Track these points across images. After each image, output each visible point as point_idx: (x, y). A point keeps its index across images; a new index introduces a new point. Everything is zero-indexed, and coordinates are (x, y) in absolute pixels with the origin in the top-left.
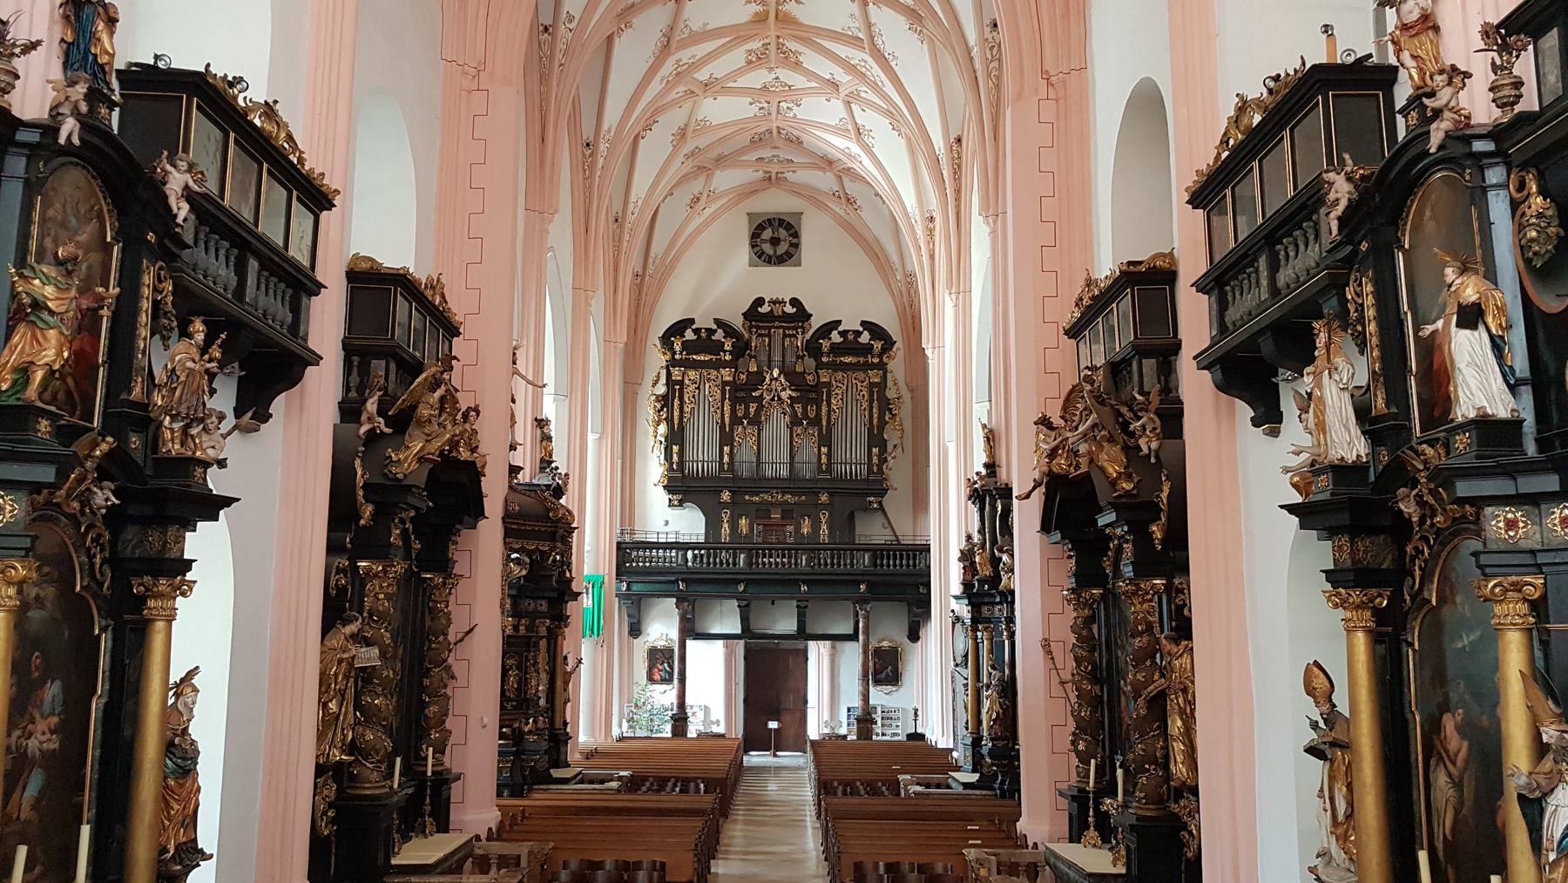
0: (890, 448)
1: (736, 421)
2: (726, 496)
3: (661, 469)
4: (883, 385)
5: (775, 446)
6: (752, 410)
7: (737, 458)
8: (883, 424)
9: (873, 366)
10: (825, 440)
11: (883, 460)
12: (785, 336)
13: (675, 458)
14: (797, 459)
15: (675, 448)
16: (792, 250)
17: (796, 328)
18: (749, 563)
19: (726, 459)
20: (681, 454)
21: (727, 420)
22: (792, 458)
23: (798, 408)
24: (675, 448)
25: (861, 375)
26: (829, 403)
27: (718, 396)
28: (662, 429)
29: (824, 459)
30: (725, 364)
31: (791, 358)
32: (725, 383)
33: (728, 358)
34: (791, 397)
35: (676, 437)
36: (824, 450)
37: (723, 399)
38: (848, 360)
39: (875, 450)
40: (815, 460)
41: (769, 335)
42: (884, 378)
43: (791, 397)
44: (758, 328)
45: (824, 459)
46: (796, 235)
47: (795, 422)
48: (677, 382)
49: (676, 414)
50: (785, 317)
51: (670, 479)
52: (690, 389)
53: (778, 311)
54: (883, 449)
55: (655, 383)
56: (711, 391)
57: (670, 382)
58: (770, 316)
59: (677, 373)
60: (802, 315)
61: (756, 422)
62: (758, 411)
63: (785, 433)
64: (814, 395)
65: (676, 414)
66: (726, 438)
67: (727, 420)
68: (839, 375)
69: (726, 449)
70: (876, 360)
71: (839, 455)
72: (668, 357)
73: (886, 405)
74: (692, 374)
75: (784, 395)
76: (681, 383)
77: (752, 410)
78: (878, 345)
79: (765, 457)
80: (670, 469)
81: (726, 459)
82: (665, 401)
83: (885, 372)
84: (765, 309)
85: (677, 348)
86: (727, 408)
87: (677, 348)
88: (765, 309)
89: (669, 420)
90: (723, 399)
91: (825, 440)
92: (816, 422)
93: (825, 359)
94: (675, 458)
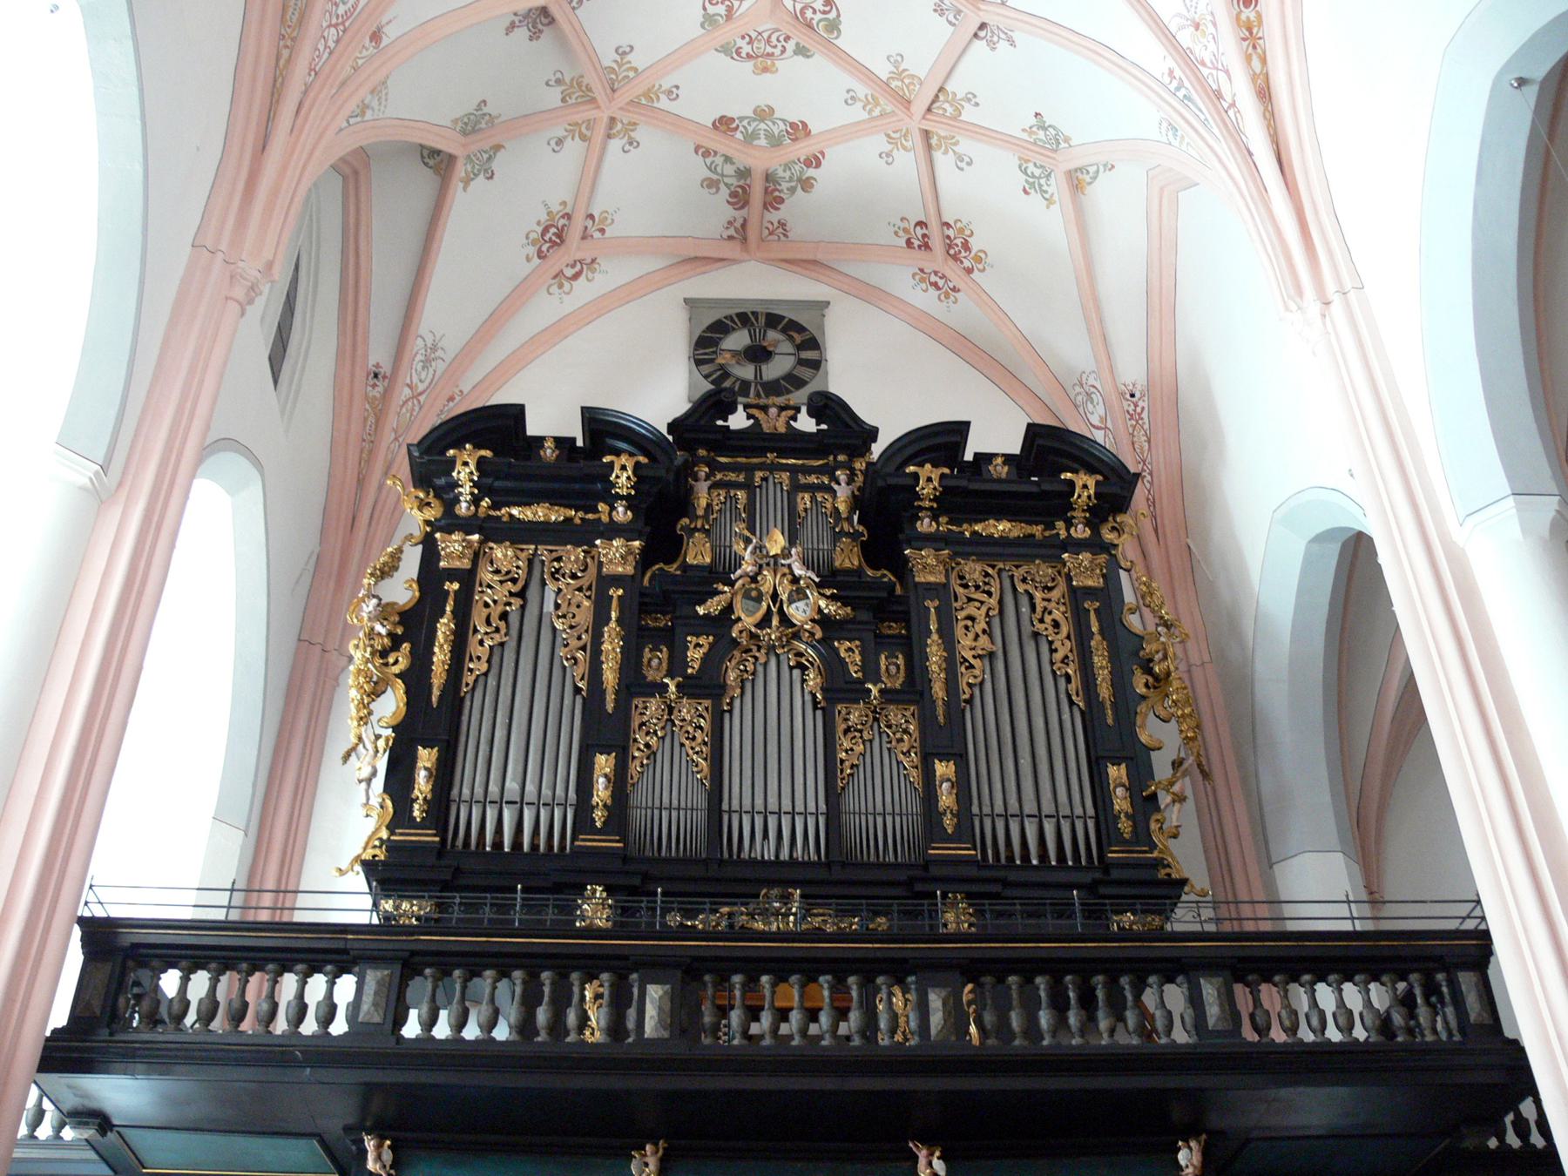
0: (1161, 765)
1: (635, 684)
2: (595, 908)
3: (371, 824)
4: (1108, 595)
5: (775, 763)
6: (695, 656)
7: (640, 797)
8: (1126, 703)
9: (1076, 546)
10: (944, 738)
11: (1146, 804)
12: (796, 488)
13: (422, 784)
14: (851, 802)
15: (426, 757)
16: (804, 372)
17: (830, 471)
18: (682, 1016)
19: (601, 791)
20: (444, 775)
21: (610, 676)
22: (833, 795)
23: (850, 653)
24: (426, 757)
25: (1044, 571)
26: (949, 642)
27: (584, 616)
28: (391, 704)
29: (946, 798)
30: (612, 531)
31: (815, 534)
32: (606, 581)
33: (622, 514)
34: (823, 620)
35: (432, 724)
36: (943, 769)
37: (601, 618)
38: (1002, 527)
39: (1116, 772)
40: (914, 806)
41: (748, 486)
42: (1111, 580)
43: (823, 620)
44: (714, 467)
45: (946, 798)
46: (813, 344)
47: (840, 689)
48: (452, 574)
49: (441, 656)
50: (794, 443)
51: (391, 847)
52: (492, 593)
53: (774, 422)
54: (1139, 760)
55: (386, 572)
56: (563, 603)
57: (430, 575)
58: (754, 442)
59: (453, 548)
60: (844, 430)
61: (705, 686)
62: (713, 661)
63: (805, 727)
64: (894, 629)
65: (441, 656)
66: (604, 729)
67: (610, 676)
68: (973, 569)
69: (604, 763)
70: (1081, 532)
71: (994, 796)
72: (433, 513)
73: (1130, 653)
74: (501, 553)
75: (799, 613)
76: (468, 578)
77: (695, 656)
78: (1085, 485)
79: (738, 791)
80: (400, 818)
81: (601, 791)
82: (412, 626)
83: (1114, 564)
84: (738, 420)
85: (464, 474)
86: (612, 645)
87: (464, 474)
88: (738, 420)
89: (416, 680)
90: (601, 618)
91: (944, 738)
92: (914, 690)
93: (925, 525)
94: (422, 784)
